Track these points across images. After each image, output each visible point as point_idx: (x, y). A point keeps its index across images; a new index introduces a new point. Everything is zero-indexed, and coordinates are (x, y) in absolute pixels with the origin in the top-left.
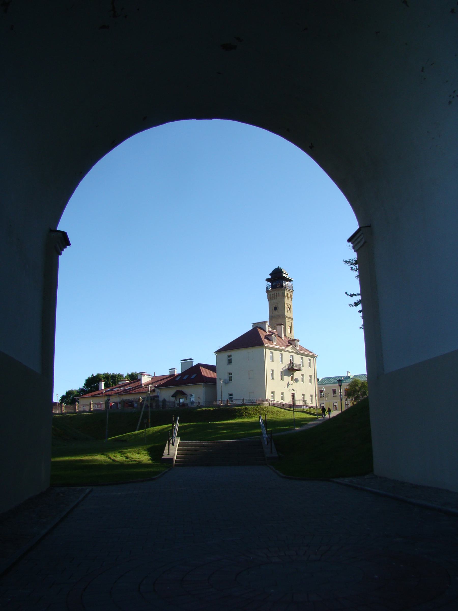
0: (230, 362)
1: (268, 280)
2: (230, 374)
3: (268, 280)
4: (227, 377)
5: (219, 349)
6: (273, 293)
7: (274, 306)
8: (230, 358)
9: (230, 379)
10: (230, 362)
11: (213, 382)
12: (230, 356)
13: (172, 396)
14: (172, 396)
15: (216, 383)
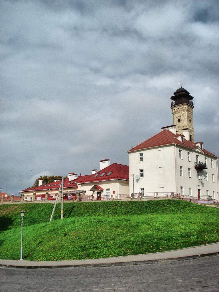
0: (142, 159)
1: (172, 98)
2: (142, 170)
3: (172, 98)
4: (139, 173)
5: (131, 148)
6: (177, 108)
7: (178, 118)
8: (142, 156)
9: (142, 175)
10: (142, 159)
11: (126, 179)
12: (142, 154)
13: (91, 190)
14: (91, 190)
15: (129, 179)
